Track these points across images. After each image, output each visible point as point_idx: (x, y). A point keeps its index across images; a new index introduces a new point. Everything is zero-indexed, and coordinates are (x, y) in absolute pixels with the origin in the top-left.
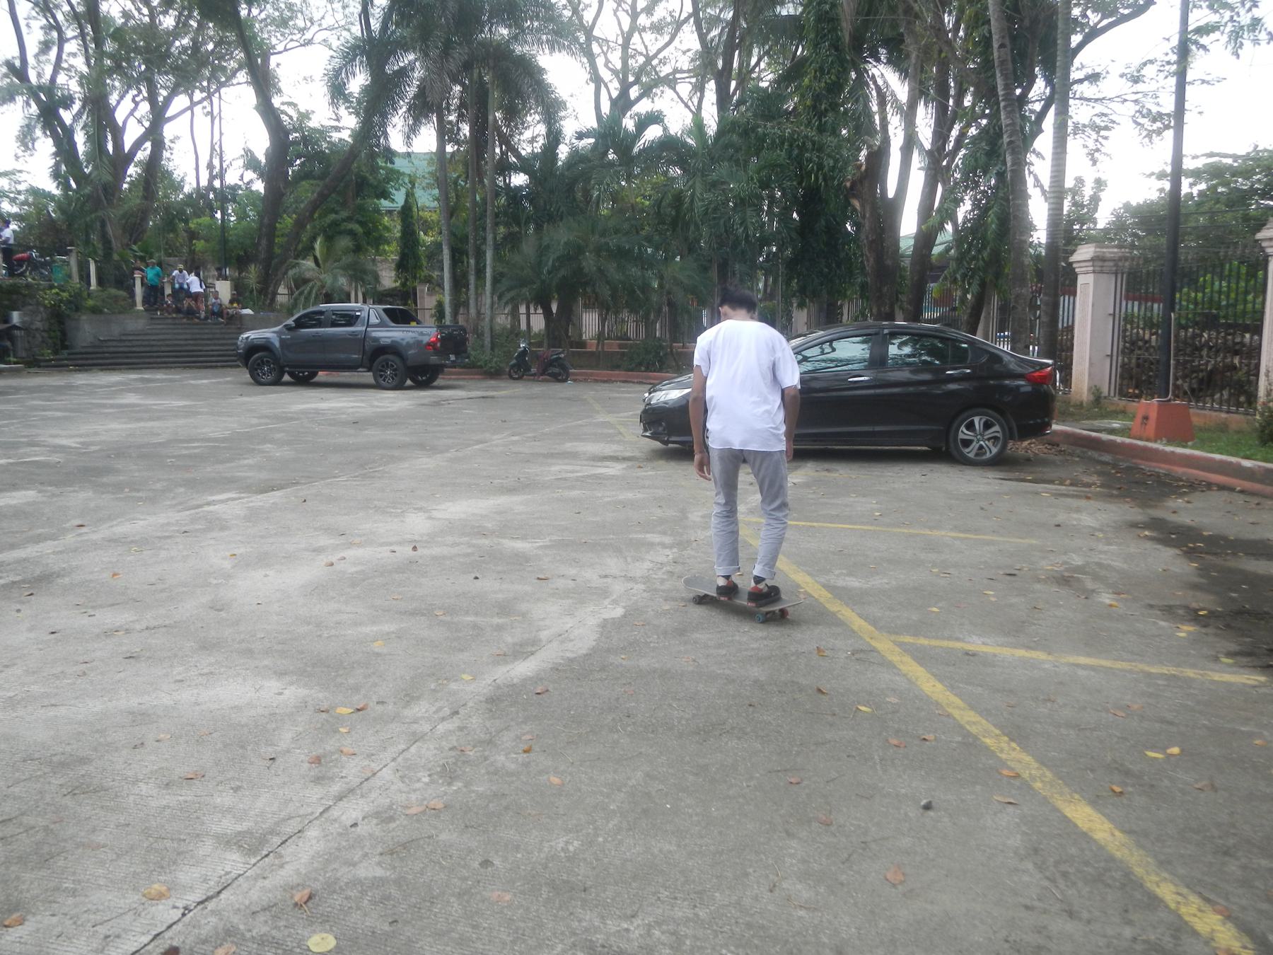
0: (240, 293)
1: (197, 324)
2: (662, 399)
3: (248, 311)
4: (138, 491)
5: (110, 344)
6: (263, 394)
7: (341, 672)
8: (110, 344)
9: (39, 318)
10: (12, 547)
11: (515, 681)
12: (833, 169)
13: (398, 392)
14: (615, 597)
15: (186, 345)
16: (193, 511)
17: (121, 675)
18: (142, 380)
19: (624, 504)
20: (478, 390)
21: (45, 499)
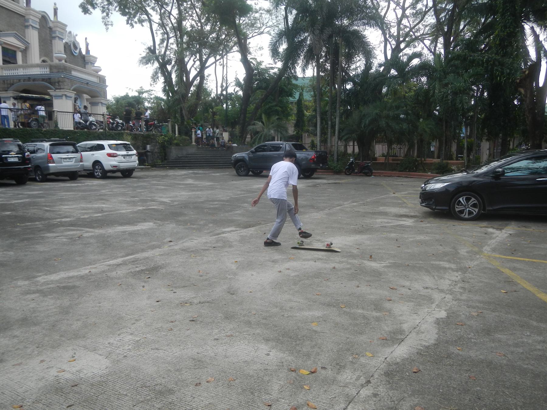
1: (216, 150)
2: (432, 188)
3: (235, 145)
4: (194, 225)
6: (242, 180)
7: (298, 342)
8: (183, 158)
9: (157, 147)
10: (143, 250)
11: (398, 360)
14: (437, 303)
16: (217, 236)
17: (189, 331)
19: (421, 243)
20: (332, 179)
21: (156, 227)
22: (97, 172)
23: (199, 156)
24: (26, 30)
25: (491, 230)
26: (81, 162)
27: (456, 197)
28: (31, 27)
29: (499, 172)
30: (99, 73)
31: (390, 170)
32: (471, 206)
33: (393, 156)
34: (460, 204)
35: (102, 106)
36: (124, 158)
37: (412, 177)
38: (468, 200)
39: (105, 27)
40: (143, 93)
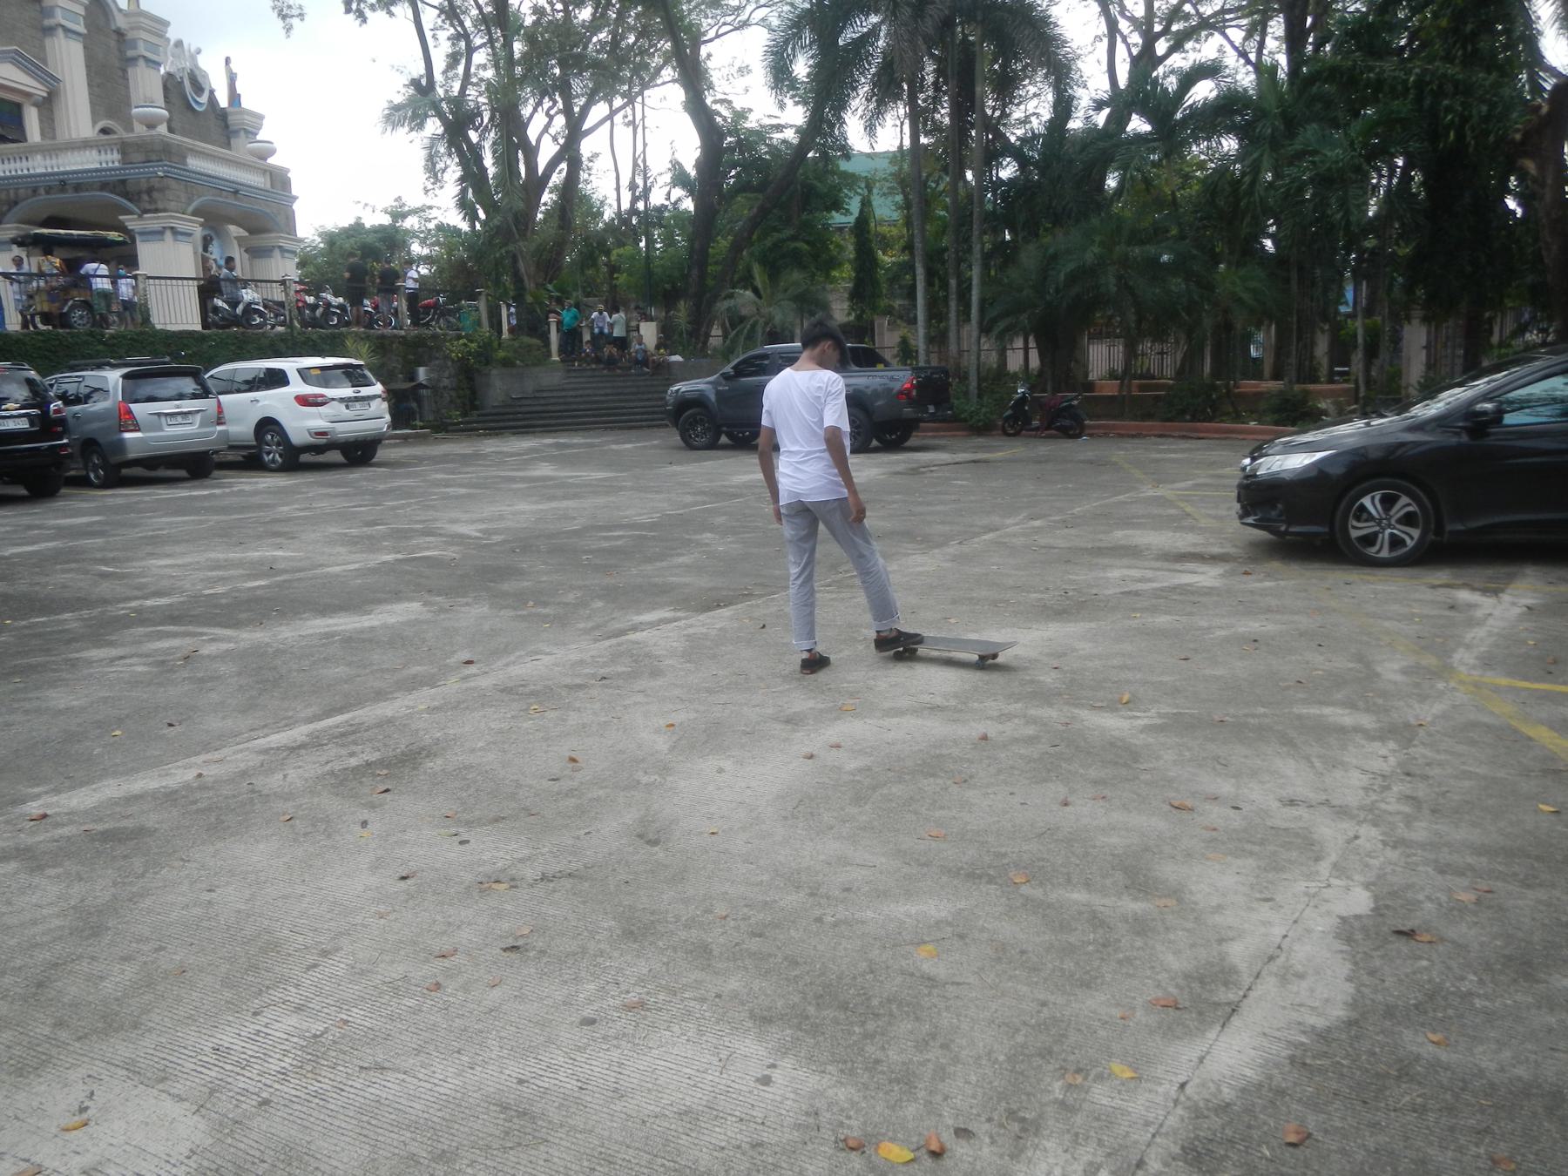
0: (667, 338)
2: (1275, 468)
3: (677, 358)
4: (545, 604)
5: (524, 402)
7: (871, 1026)
8: (524, 402)
9: (446, 374)
10: (380, 696)
11: (1228, 1094)
12: (1486, 119)
13: (862, 456)
14: (1333, 858)
15: (607, 401)
16: (614, 641)
17: (496, 994)
18: (557, 446)
20: (964, 451)
21: (429, 616)
22: (269, 453)
23: (571, 393)
24: (48, 42)
25: (1464, 595)
26: (219, 424)
27: (1352, 493)
28: (60, 32)
29: (1485, 413)
30: (271, 161)
31: (1135, 418)
32: (1399, 521)
33: (1141, 377)
34: (1365, 516)
35: (283, 257)
36: (347, 407)
37: (1201, 435)
38: (1388, 502)
39: (280, 23)
40: (404, 216)
